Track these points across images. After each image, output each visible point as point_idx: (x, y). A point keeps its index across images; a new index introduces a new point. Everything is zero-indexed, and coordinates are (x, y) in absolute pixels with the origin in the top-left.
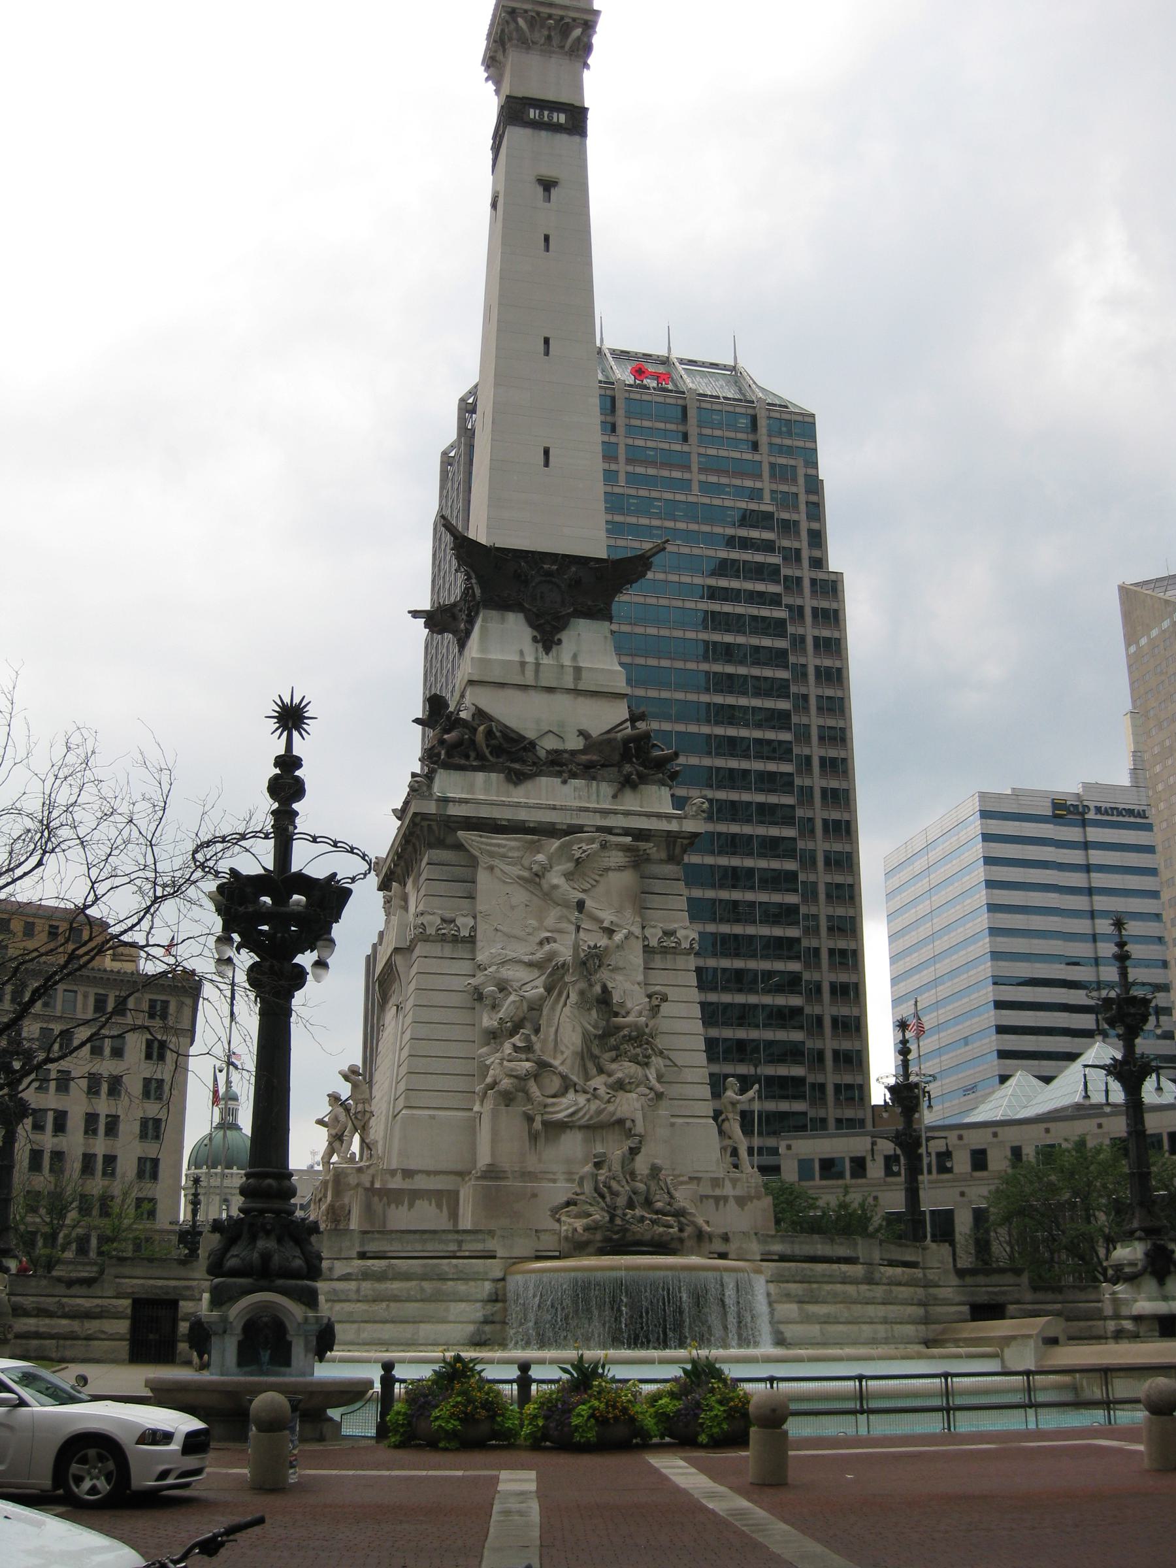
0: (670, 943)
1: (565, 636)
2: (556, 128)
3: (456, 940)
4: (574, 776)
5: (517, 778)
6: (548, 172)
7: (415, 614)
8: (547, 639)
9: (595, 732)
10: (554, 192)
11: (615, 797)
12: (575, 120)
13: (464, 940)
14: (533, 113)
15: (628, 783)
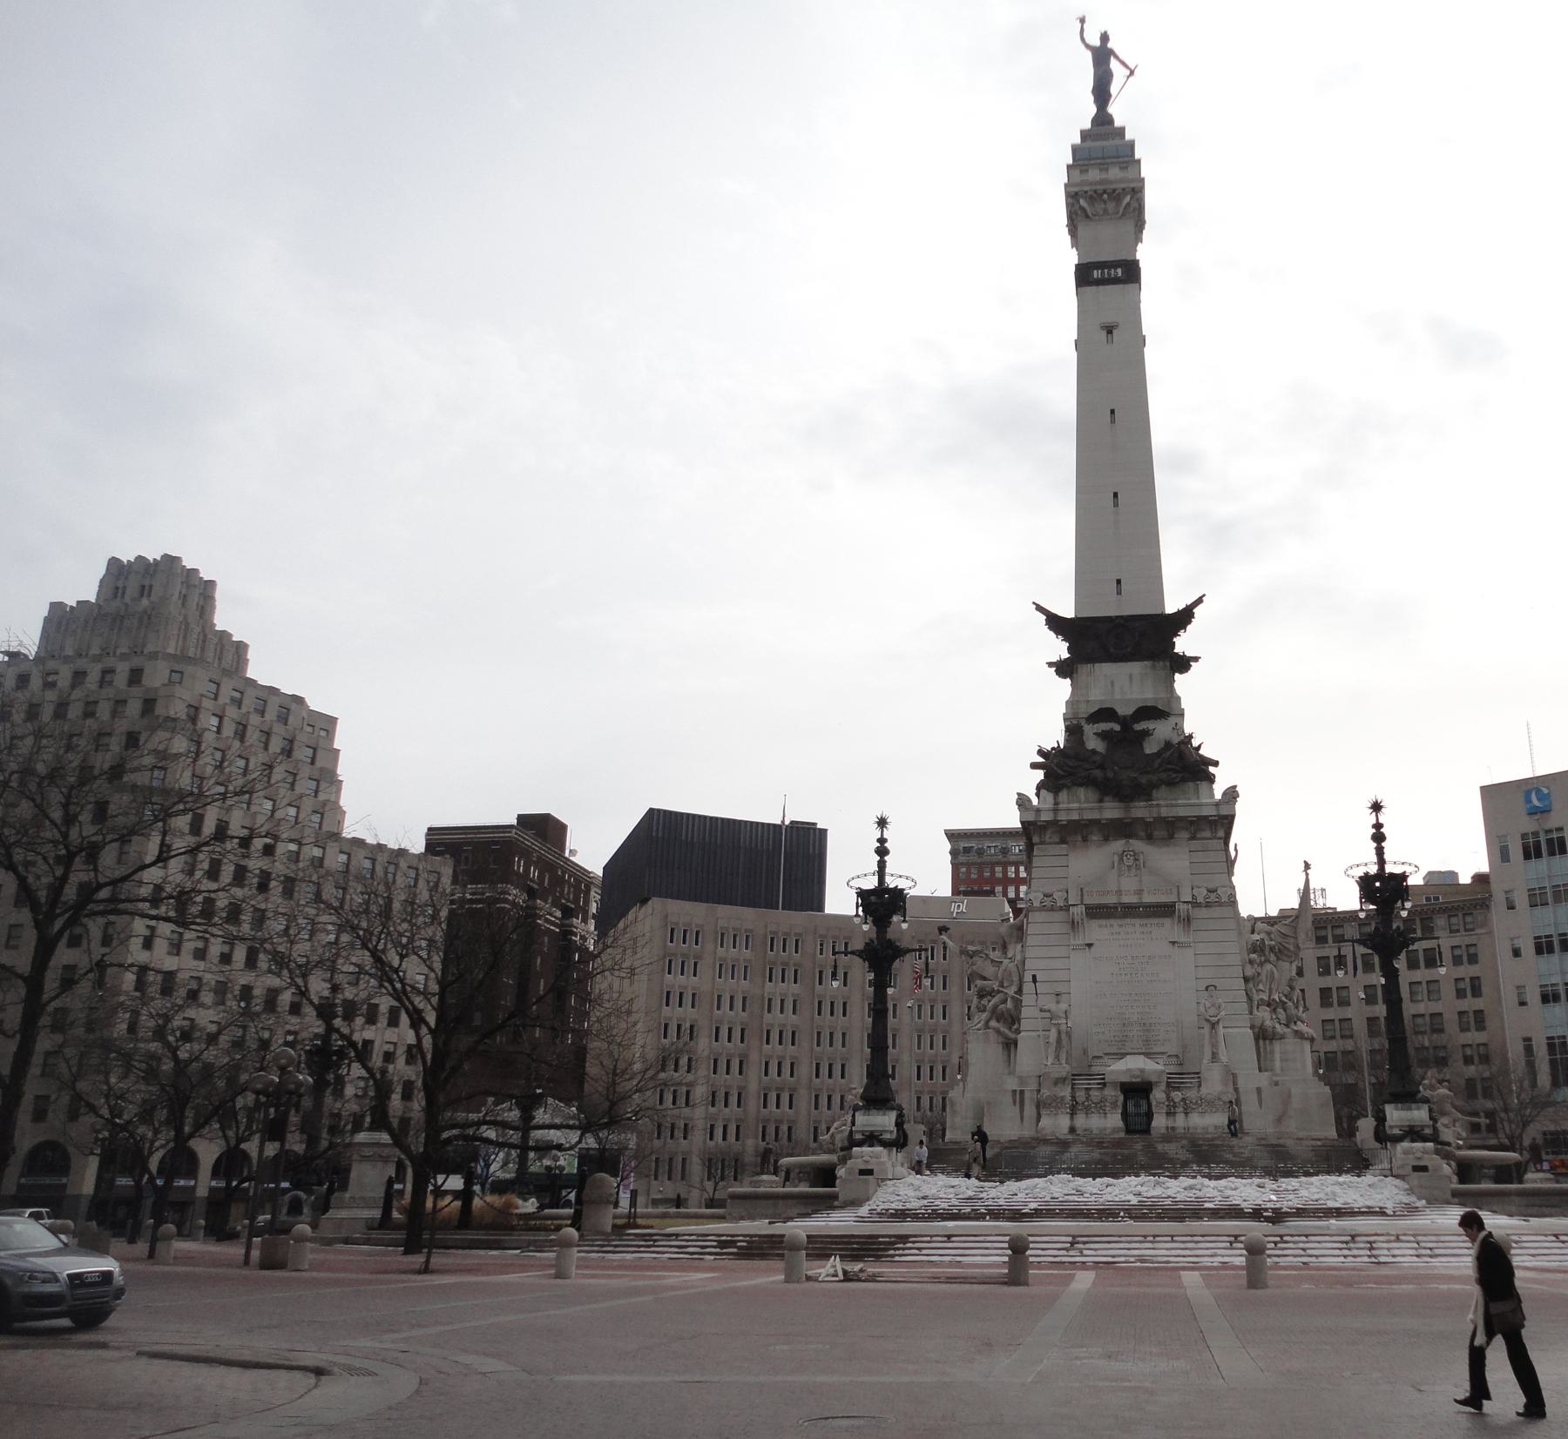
0: (1213, 897)
2: (1115, 281)
3: (1052, 909)
6: (1109, 319)
7: (1050, 664)
12: (1130, 273)
13: (1061, 909)
14: (1096, 274)
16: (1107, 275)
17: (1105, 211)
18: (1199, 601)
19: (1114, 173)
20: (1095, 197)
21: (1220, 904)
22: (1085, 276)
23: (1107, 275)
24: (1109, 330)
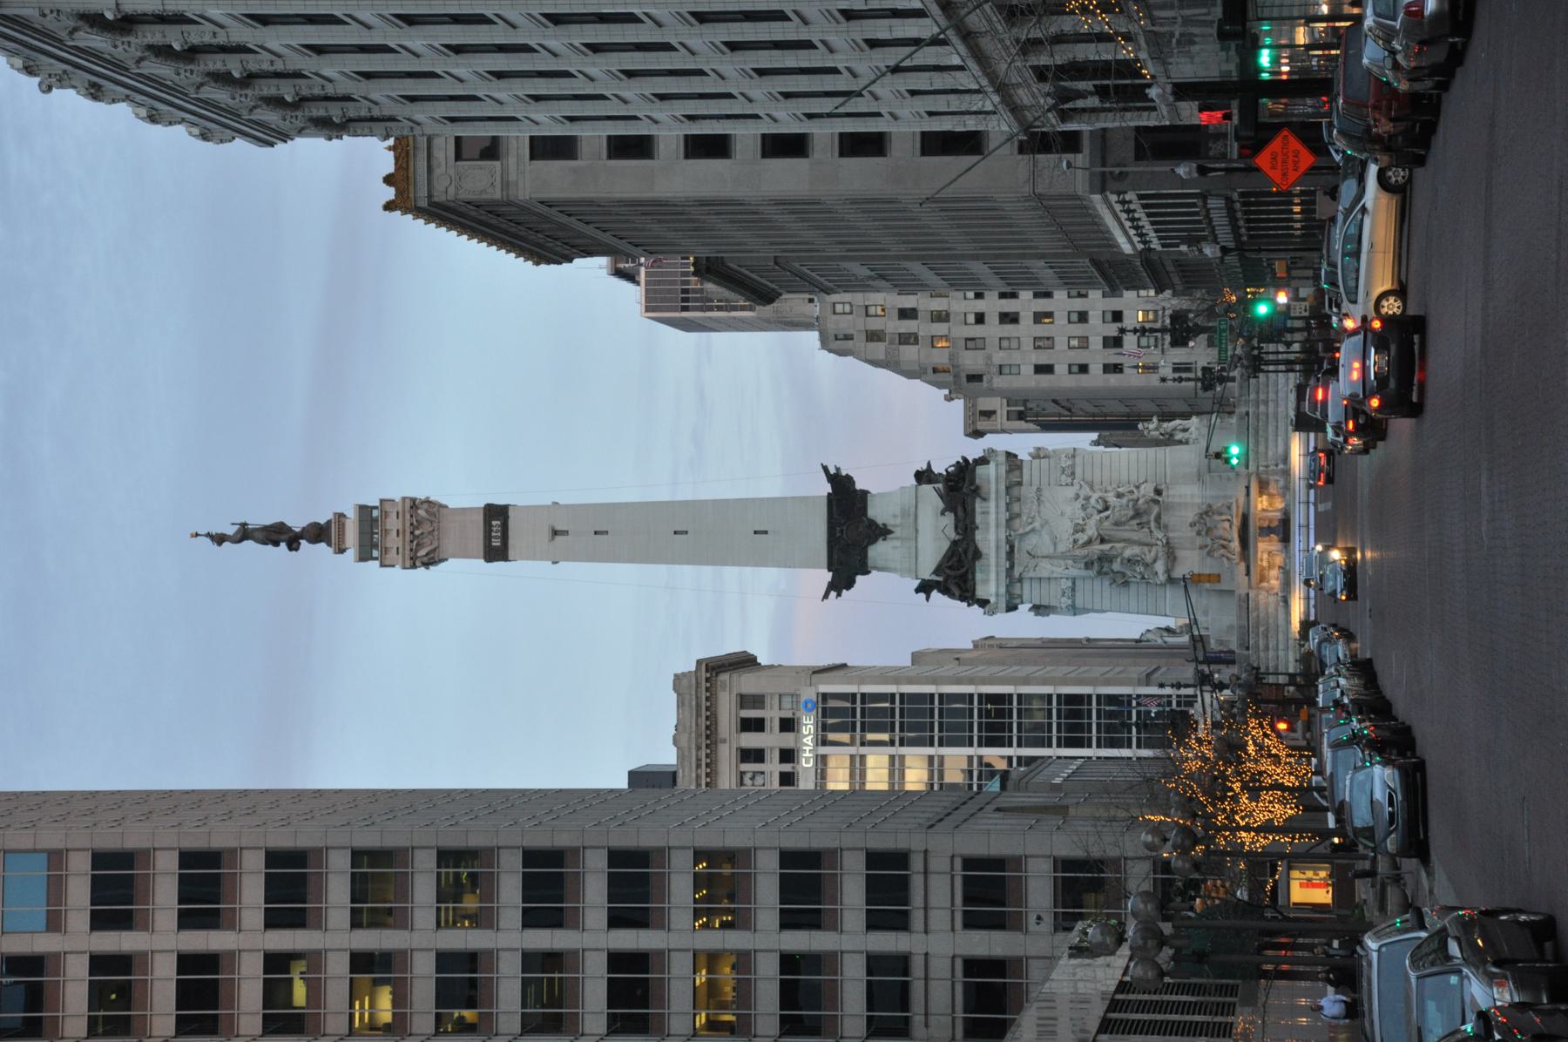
0: (1068, 471)
1: (880, 522)
3: (1073, 590)
4: (973, 522)
5: (977, 554)
6: (547, 533)
8: (883, 532)
9: (941, 505)
10: (558, 528)
11: (985, 499)
12: (496, 514)
15: (976, 492)
16: (496, 533)
17: (431, 533)
18: (825, 469)
19: (393, 523)
20: (416, 540)
21: (1073, 466)
22: (496, 551)
23: (496, 533)
24: (555, 533)
